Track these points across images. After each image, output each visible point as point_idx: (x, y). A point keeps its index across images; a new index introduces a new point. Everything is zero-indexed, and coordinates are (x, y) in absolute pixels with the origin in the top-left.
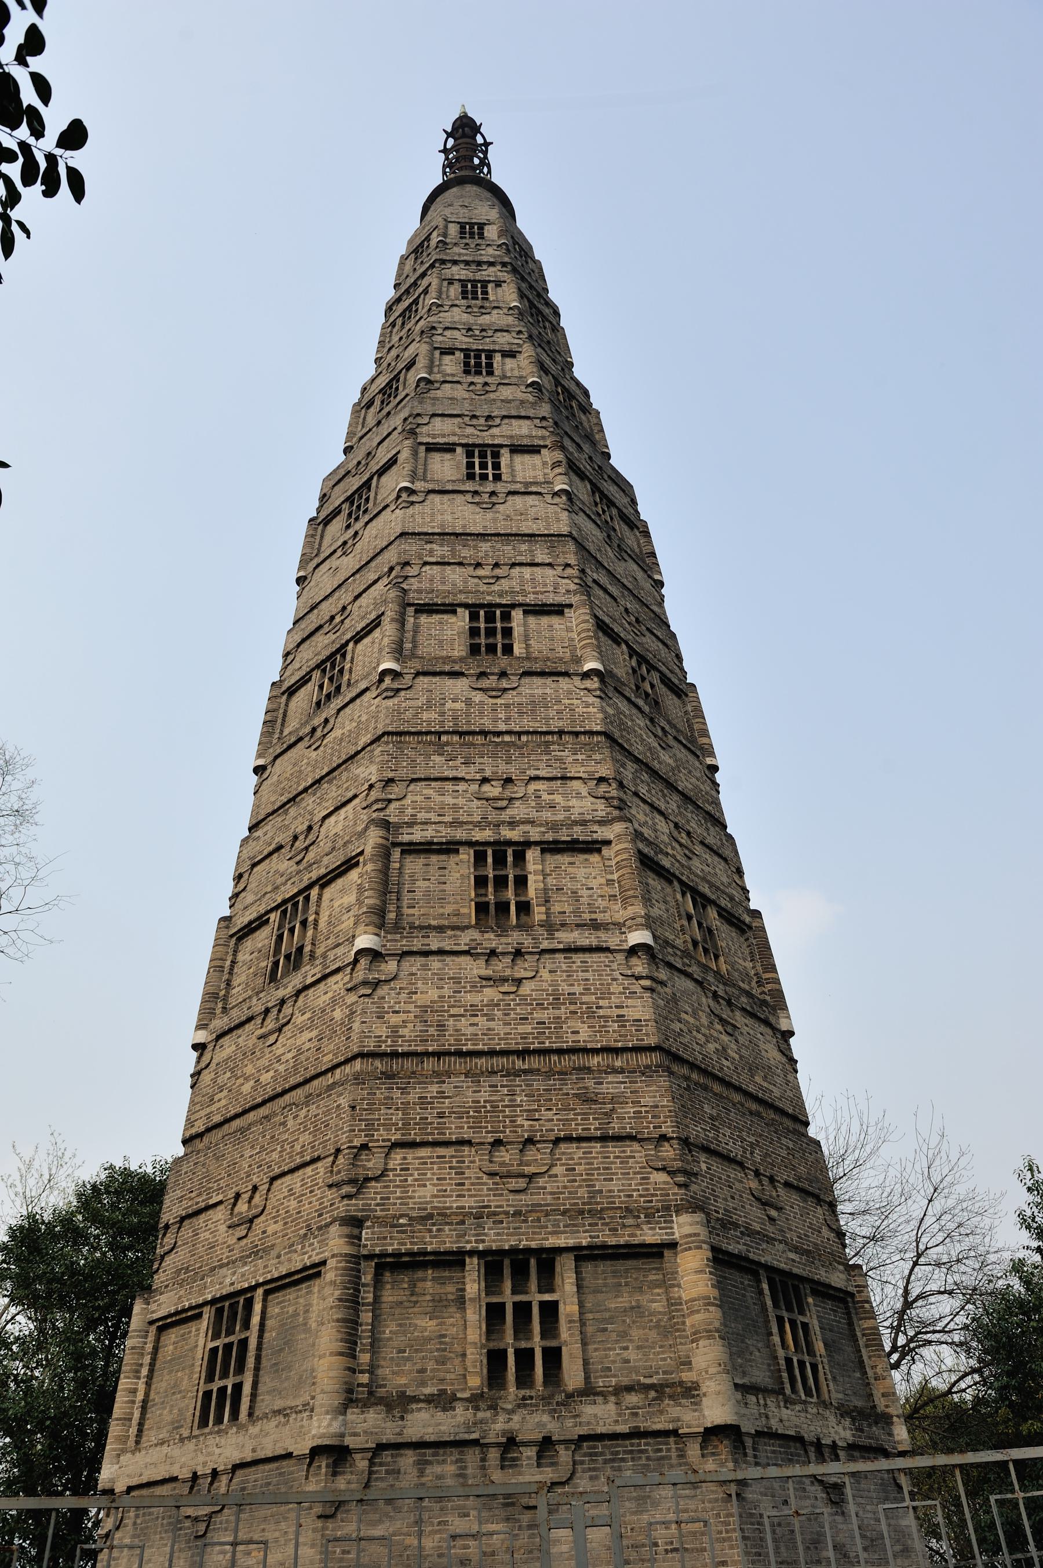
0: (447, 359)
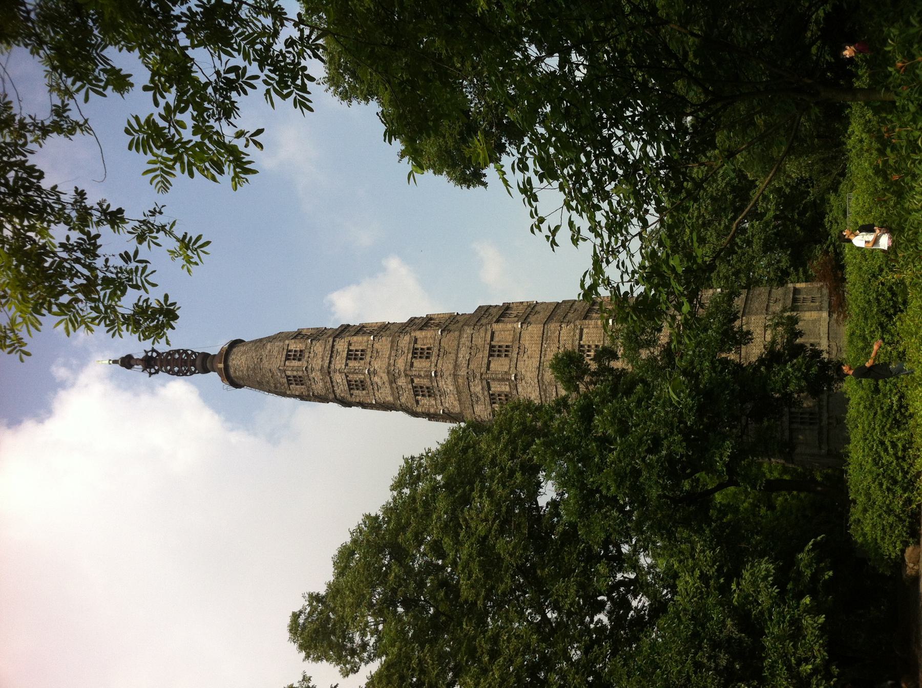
0: (415, 364)
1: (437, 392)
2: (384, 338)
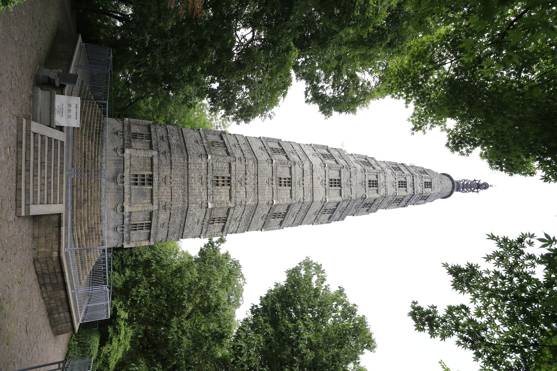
0: (375, 177)
2: (392, 194)
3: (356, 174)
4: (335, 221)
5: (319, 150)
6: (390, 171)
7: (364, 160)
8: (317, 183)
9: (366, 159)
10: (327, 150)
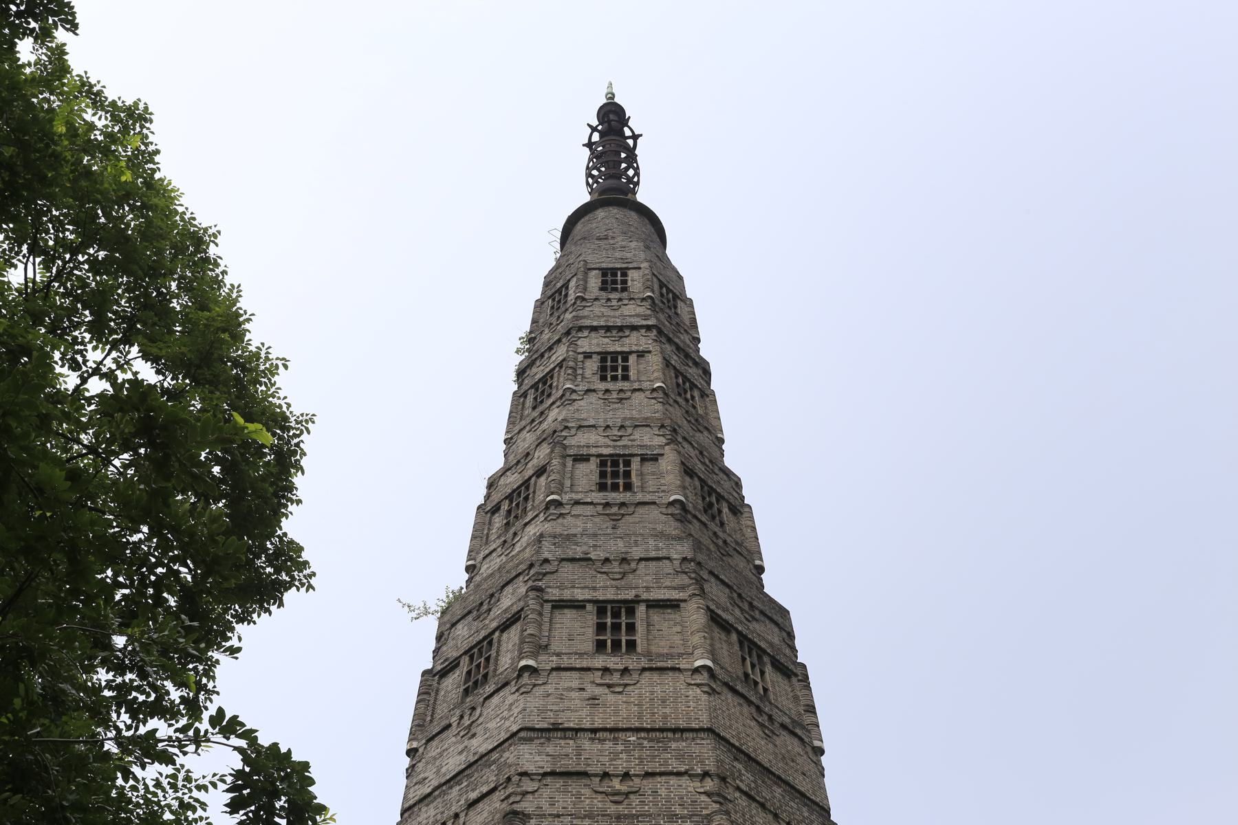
0: (583, 468)
1: (512, 531)
2: (659, 407)
3: (569, 538)
4: (794, 650)
5: (442, 709)
6: (553, 414)
7: (498, 521)
8: (619, 708)
9: (496, 509)
10: (443, 674)
